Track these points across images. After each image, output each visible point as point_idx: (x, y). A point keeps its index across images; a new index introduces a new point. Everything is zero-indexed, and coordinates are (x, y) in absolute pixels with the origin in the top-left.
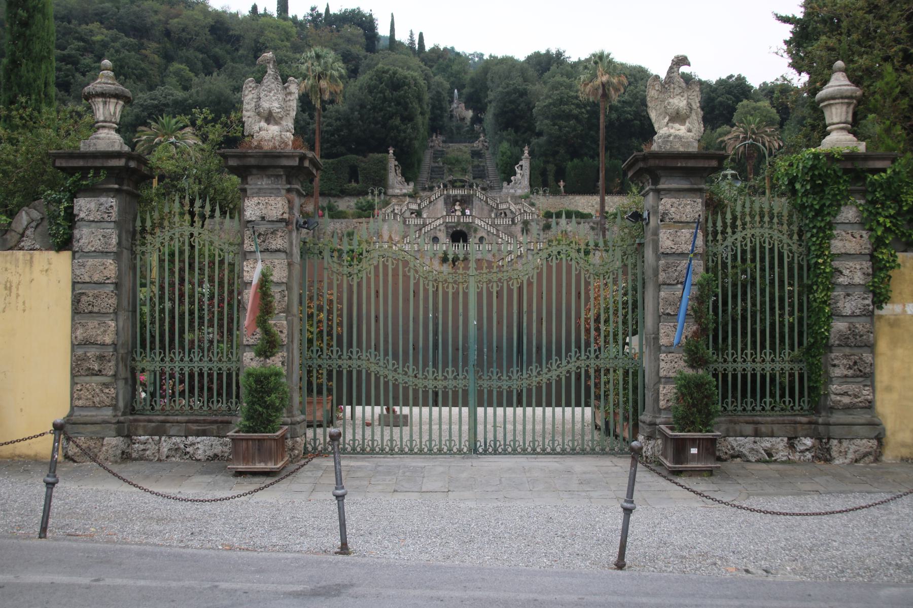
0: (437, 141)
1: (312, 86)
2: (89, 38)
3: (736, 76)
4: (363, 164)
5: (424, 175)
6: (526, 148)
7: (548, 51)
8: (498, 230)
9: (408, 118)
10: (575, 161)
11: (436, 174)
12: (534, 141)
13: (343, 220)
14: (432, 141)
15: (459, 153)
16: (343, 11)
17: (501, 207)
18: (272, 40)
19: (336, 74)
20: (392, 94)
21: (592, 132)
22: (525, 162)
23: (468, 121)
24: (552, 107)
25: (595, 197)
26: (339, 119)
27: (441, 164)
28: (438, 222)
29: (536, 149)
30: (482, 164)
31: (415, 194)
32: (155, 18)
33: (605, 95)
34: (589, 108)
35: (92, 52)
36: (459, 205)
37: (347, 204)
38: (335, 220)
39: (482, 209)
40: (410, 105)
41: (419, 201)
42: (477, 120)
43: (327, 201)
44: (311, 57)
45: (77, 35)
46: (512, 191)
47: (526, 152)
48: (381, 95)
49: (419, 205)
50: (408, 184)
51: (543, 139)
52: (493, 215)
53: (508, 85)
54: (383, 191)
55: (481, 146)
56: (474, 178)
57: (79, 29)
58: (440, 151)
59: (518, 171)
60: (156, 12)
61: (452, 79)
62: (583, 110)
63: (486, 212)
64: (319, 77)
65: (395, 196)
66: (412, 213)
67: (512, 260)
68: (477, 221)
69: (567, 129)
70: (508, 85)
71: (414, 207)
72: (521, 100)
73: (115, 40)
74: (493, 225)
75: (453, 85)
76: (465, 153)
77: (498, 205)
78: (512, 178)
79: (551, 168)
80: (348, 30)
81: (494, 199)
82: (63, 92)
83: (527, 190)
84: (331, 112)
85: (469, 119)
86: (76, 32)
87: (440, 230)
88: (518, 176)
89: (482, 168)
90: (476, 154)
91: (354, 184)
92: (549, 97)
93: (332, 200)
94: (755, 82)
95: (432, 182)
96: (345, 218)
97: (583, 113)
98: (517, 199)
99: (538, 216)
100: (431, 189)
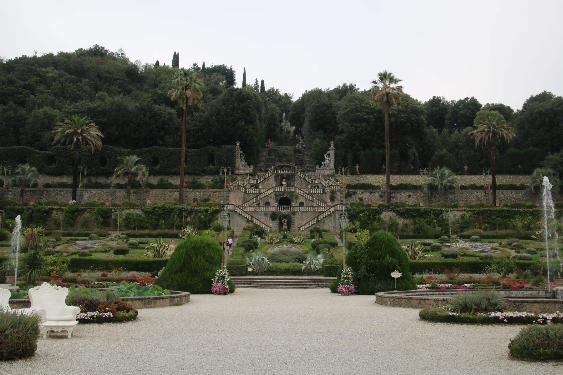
0: (272, 144)
1: (181, 94)
2: (44, 75)
3: (470, 98)
4: (218, 153)
5: (262, 164)
6: (332, 142)
7: (344, 85)
8: (313, 197)
9: (250, 122)
10: (367, 151)
11: (269, 163)
12: (338, 137)
13: (201, 190)
14: (268, 144)
15: (287, 151)
16: (214, 66)
17: (315, 182)
18: (165, 79)
19: (198, 86)
20: (239, 105)
21: (377, 131)
22: (331, 152)
23: (292, 134)
24: (349, 114)
25: (381, 176)
26: (202, 122)
27: (274, 157)
28: (269, 192)
29: (339, 142)
30: (301, 157)
31: (254, 173)
32: (90, 65)
33: (389, 103)
34: (375, 115)
35: (45, 84)
36: (285, 181)
37: (206, 180)
38: (196, 190)
39: (302, 184)
40: (252, 112)
41: (256, 178)
42: (297, 132)
43: (192, 178)
44: (181, 75)
45: (36, 73)
46: (322, 172)
47: (332, 145)
48: (232, 106)
49: (257, 181)
50: (249, 167)
51: (344, 135)
52: (309, 187)
53: (319, 102)
54: (230, 170)
55: (300, 147)
56: (295, 165)
57: (38, 69)
58: (273, 149)
59: (327, 158)
60: (91, 62)
61: (282, 108)
62: (371, 116)
63: (304, 186)
64: (186, 88)
65: (240, 175)
66: (252, 186)
67: (324, 218)
68: (298, 191)
69: (360, 129)
70: (319, 102)
71: (254, 182)
72: (328, 111)
73: (61, 76)
74: (309, 194)
75: (283, 111)
76: (290, 150)
77: (312, 180)
78: (323, 163)
79: (350, 156)
80: (216, 77)
81: (310, 177)
82: (16, 105)
83: (333, 171)
84: (197, 117)
85: (293, 132)
86: (36, 71)
87: (271, 197)
88: (327, 161)
89: (301, 159)
90: (297, 151)
91: (211, 167)
92: (347, 107)
93: (196, 178)
94: (483, 101)
95: (267, 168)
96: (203, 189)
97: (371, 117)
98: (326, 177)
99: (342, 188)
100: (266, 171)
